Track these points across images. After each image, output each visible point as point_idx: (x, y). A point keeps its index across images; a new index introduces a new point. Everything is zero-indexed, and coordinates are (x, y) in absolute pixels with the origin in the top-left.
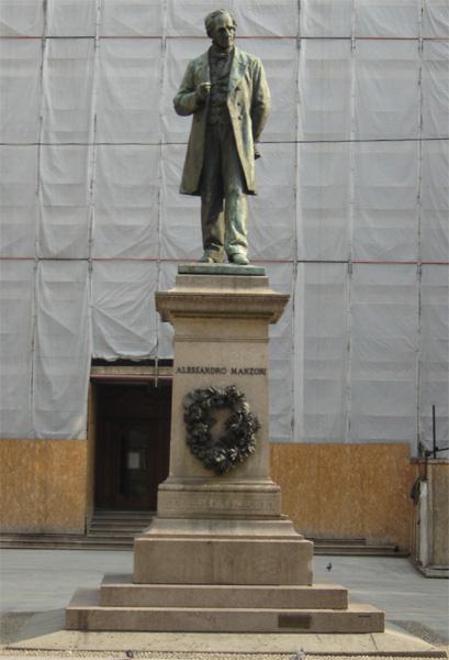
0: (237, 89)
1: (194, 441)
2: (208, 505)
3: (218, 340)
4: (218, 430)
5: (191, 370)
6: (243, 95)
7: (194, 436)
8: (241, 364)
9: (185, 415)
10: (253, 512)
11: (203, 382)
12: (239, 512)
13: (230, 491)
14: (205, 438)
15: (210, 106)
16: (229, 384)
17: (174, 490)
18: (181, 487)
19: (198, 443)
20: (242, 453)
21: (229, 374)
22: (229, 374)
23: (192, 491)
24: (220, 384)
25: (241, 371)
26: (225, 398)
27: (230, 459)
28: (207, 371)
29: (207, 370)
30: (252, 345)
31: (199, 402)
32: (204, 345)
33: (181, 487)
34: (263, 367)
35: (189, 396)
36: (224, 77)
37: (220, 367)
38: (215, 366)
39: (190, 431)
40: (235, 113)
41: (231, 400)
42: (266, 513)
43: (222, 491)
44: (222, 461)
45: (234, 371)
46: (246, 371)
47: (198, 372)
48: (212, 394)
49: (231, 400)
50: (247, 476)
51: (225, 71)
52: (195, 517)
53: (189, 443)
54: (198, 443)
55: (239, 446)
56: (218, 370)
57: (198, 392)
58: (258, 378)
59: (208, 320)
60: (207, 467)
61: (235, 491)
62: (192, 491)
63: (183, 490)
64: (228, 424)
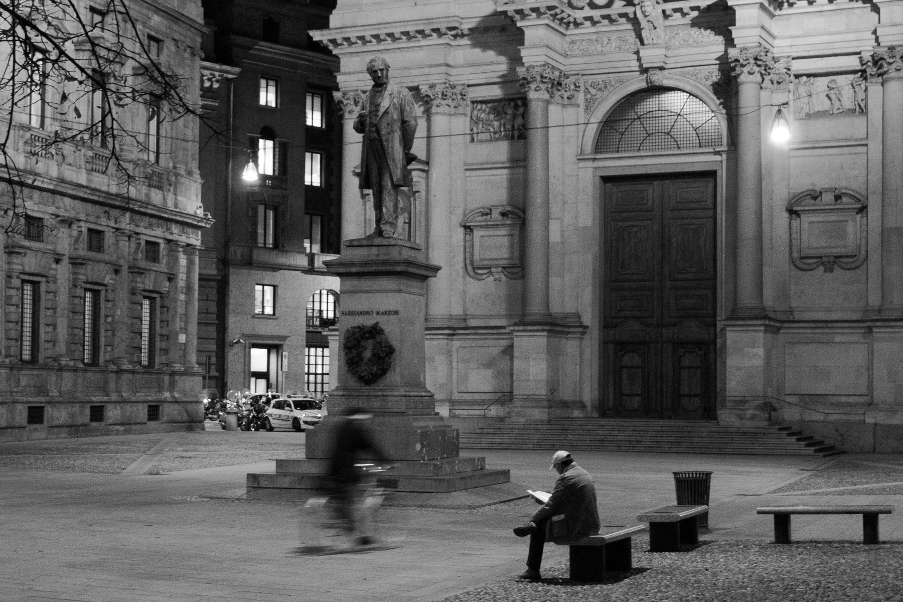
0: (386, 112)
4: (367, 354)
5: (351, 313)
6: (392, 117)
8: (382, 309)
16: (375, 322)
18: (341, 393)
21: (374, 315)
22: (374, 315)
24: (369, 322)
26: (370, 332)
27: (371, 374)
28: (361, 313)
29: (361, 313)
30: (390, 294)
31: (354, 334)
34: (397, 309)
38: (366, 310)
41: (375, 331)
42: (395, 410)
44: (365, 376)
45: (378, 313)
46: (386, 313)
47: (355, 315)
48: (361, 328)
49: (375, 331)
58: (393, 317)
61: (376, 396)
62: (349, 396)
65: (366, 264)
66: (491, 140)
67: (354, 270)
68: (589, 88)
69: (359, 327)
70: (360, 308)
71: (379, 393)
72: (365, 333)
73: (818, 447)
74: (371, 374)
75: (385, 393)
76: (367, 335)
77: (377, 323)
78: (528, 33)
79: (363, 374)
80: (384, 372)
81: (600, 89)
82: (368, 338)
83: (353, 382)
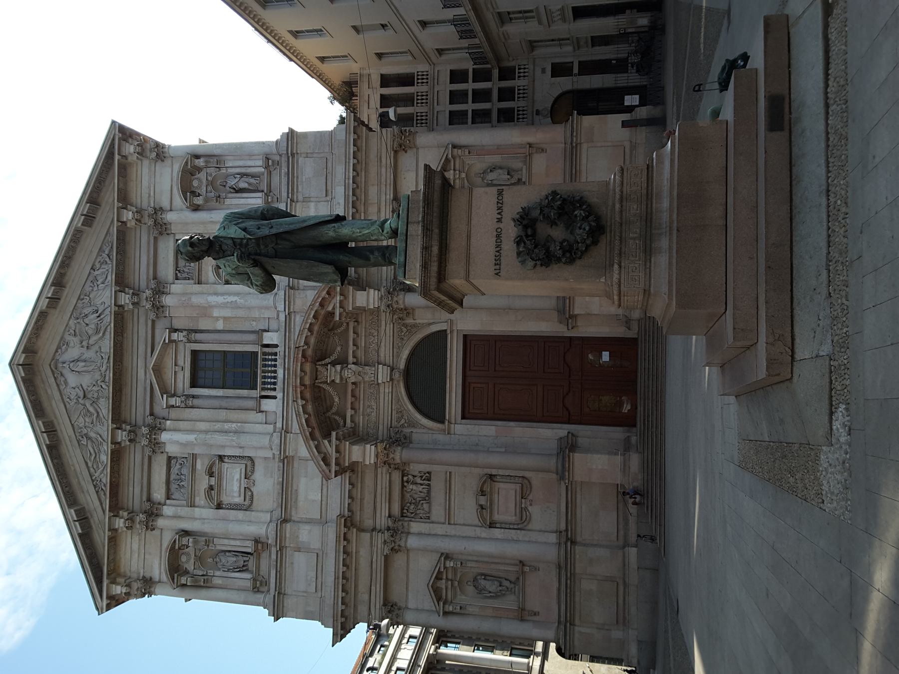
0: (245, 230)
1: (568, 255)
2: (634, 239)
3: (469, 237)
4: (558, 233)
7: (564, 255)
8: (493, 213)
10: (644, 192)
11: (509, 247)
12: (644, 207)
13: (621, 218)
14: (565, 244)
15: (260, 255)
16: (512, 224)
17: (620, 274)
18: (616, 266)
19: (570, 252)
20: (581, 206)
22: (501, 225)
23: (620, 254)
24: (511, 231)
26: (525, 227)
27: (587, 217)
28: (498, 246)
31: (529, 253)
32: (473, 251)
33: (616, 266)
35: (523, 262)
36: (234, 243)
37: (495, 233)
38: (495, 239)
39: (559, 260)
40: (266, 231)
44: (590, 225)
45: (499, 220)
48: (519, 242)
51: (230, 242)
52: (648, 251)
53: (571, 261)
54: (570, 252)
56: (498, 236)
57: (519, 254)
60: (595, 243)
61: (621, 212)
62: (620, 254)
63: (620, 267)
64: (553, 223)
65: (427, 230)
66: (429, 503)
67: (435, 250)
68: (401, 424)
69: (518, 243)
70: (492, 249)
71: (618, 206)
72: (527, 236)
73: (665, 204)
74: (587, 217)
75: (618, 196)
76: (529, 232)
77: (514, 220)
78: (354, 459)
79: (587, 228)
80: (581, 202)
81: (402, 416)
82: (534, 235)
83: (599, 252)
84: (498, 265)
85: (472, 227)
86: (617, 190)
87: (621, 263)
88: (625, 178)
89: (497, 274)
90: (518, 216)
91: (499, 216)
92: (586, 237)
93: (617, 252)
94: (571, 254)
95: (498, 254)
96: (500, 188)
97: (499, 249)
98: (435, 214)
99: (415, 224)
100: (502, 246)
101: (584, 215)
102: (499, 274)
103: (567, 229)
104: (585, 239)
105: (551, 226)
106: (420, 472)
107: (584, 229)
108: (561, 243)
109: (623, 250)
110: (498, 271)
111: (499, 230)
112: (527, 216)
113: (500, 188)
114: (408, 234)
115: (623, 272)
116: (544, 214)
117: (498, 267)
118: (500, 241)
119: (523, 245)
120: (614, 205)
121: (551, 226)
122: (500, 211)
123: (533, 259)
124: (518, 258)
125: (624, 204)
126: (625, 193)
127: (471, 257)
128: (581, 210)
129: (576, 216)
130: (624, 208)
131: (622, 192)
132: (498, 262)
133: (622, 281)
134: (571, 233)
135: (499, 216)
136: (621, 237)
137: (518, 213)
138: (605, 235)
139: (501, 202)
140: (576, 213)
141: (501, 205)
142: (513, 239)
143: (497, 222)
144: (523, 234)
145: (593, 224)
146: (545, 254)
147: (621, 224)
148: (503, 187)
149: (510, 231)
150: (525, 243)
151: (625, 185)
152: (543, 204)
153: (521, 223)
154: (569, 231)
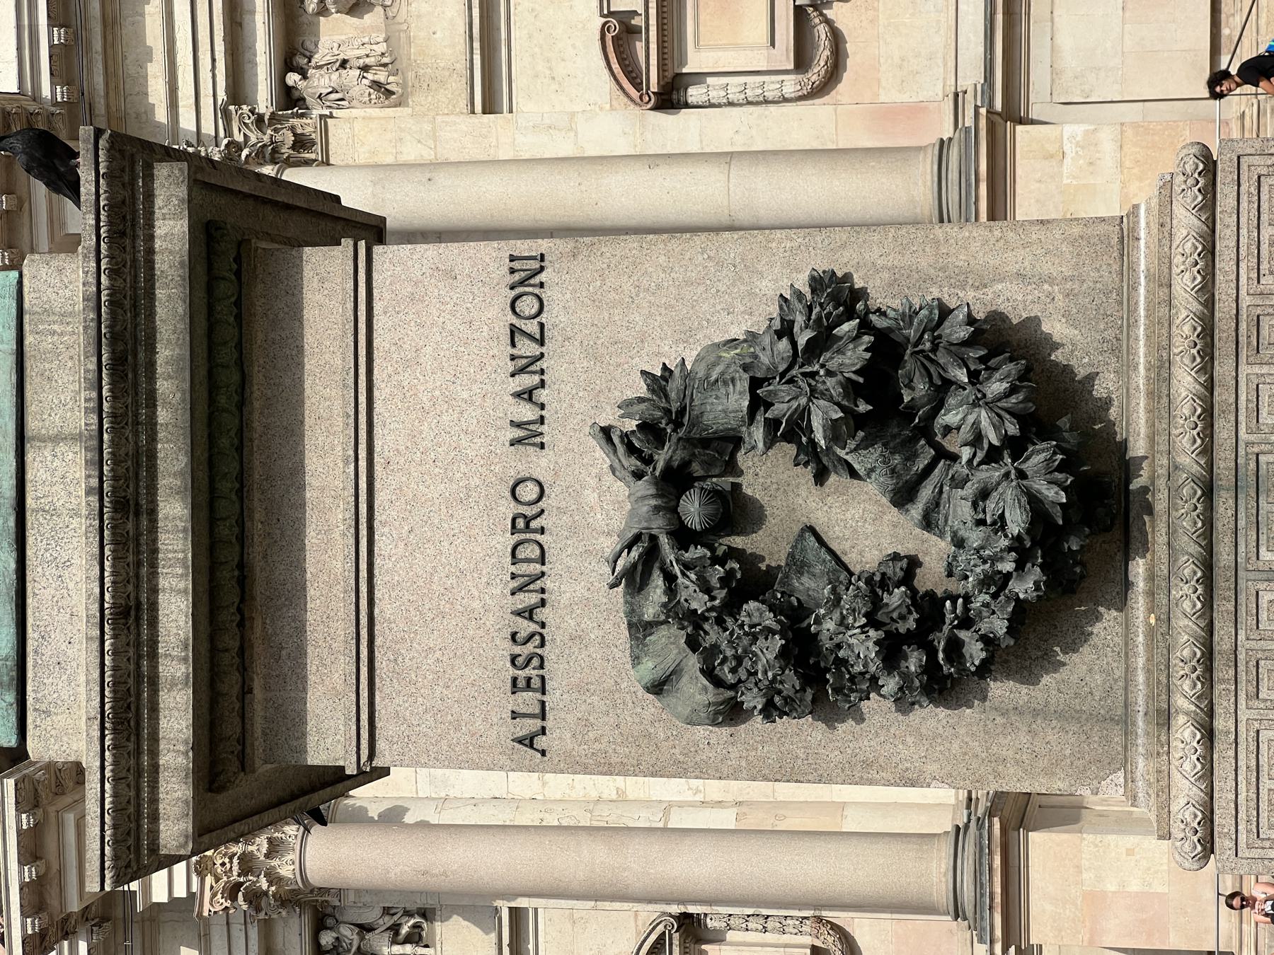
9: (770, 711)
13: (1207, 450)
16: (600, 456)
17: (1208, 774)
18: (1185, 733)
21: (539, 464)
22: (539, 464)
25: (526, 395)
27: (1016, 446)
37: (510, 509)
43: (1208, 490)
44: (1034, 503)
50: (1119, 348)
54: (920, 638)
55: (938, 405)
56: (524, 525)
57: (640, 629)
59: (259, 589)
61: (1208, 415)
63: (1209, 735)
69: (634, 579)
71: (1185, 382)
72: (683, 536)
74: (1016, 446)
75: (1185, 329)
76: (693, 509)
79: (1017, 522)
84: (528, 686)
85: (378, 469)
86: (1185, 285)
87: (1211, 713)
88: (1225, 223)
89: (528, 741)
90: (631, 425)
91: (527, 412)
92: (1007, 566)
93: (1185, 647)
94: (932, 652)
95: (526, 627)
96: (524, 247)
97: (533, 599)
98: (163, 415)
99: (62, 447)
100: (548, 583)
101: (996, 442)
102: (540, 742)
103: (903, 496)
104: (1008, 576)
105: (821, 477)
106: (387, 911)
107: (1000, 524)
108: (877, 585)
109: (1223, 641)
110: (533, 725)
111: (528, 492)
112: (678, 425)
113: (524, 247)
114: (30, 502)
115: (1223, 769)
116: (773, 425)
117: (528, 700)
118: (531, 551)
119: (658, 581)
120: (1162, 371)
121: (821, 477)
122: (528, 380)
123: (718, 682)
124: (636, 660)
125: (1223, 369)
126: (1224, 308)
127: (378, 641)
128: (975, 404)
129: (947, 429)
130: (1222, 396)
131: (1210, 304)
132: (529, 672)
133: (1223, 819)
134: (928, 522)
135: (527, 412)
136: (1208, 565)
137: (627, 405)
138: (1117, 533)
139: (532, 327)
140: (950, 417)
141: (527, 348)
142: (610, 545)
143: (514, 442)
144: (658, 525)
145: (1054, 495)
146: (783, 654)
147: (1208, 490)
148: (543, 245)
149: (591, 497)
150: (670, 578)
151: (1225, 263)
152: (765, 359)
153: (648, 461)
154: (916, 510)
